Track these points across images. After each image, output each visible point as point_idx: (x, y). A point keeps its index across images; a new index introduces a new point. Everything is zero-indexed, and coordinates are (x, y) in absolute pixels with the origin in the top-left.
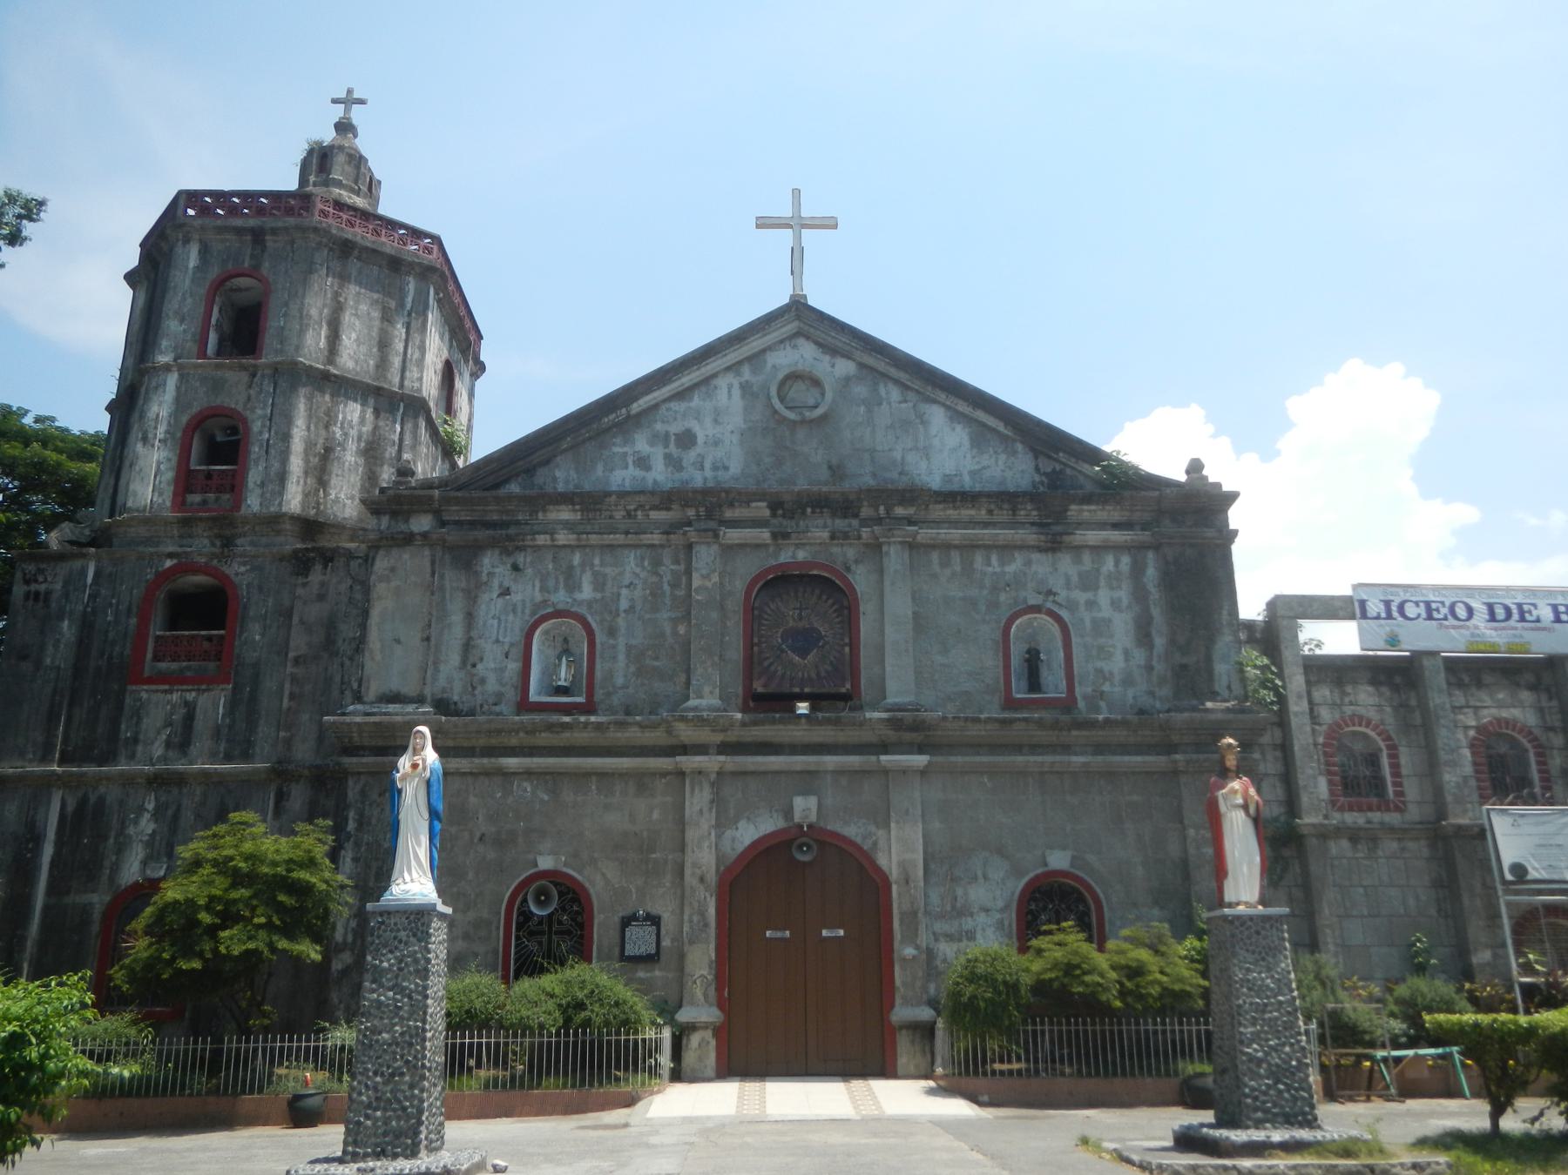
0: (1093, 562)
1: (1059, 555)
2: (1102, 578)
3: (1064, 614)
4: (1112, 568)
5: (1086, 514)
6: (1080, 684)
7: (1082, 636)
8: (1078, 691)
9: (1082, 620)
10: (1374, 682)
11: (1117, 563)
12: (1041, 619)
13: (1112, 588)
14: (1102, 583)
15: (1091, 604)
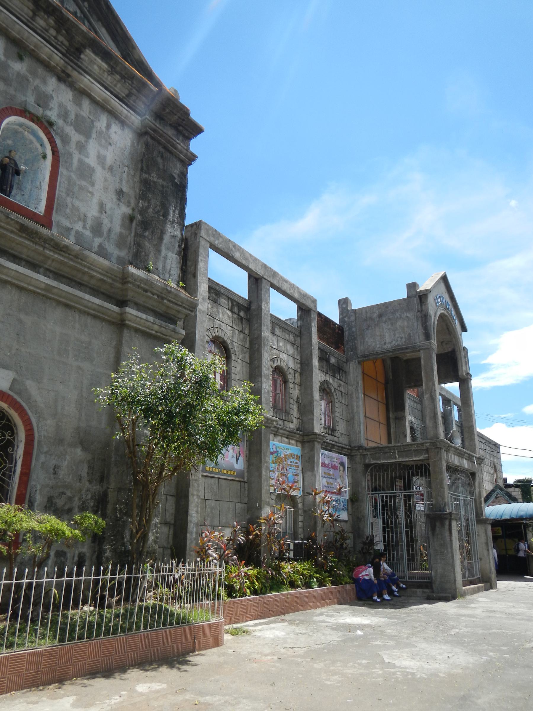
0: (90, 112)
1: (62, 86)
2: (94, 131)
3: (58, 141)
4: (104, 129)
5: (96, 67)
6: (56, 212)
7: (67, 169)
8: (55, 217)
9: (70, 155)
10: (231, 310)
11: (108, 127)
12: (34, 133)
13: (101, 145)
14: (94, 135)
15: (81, 148)
